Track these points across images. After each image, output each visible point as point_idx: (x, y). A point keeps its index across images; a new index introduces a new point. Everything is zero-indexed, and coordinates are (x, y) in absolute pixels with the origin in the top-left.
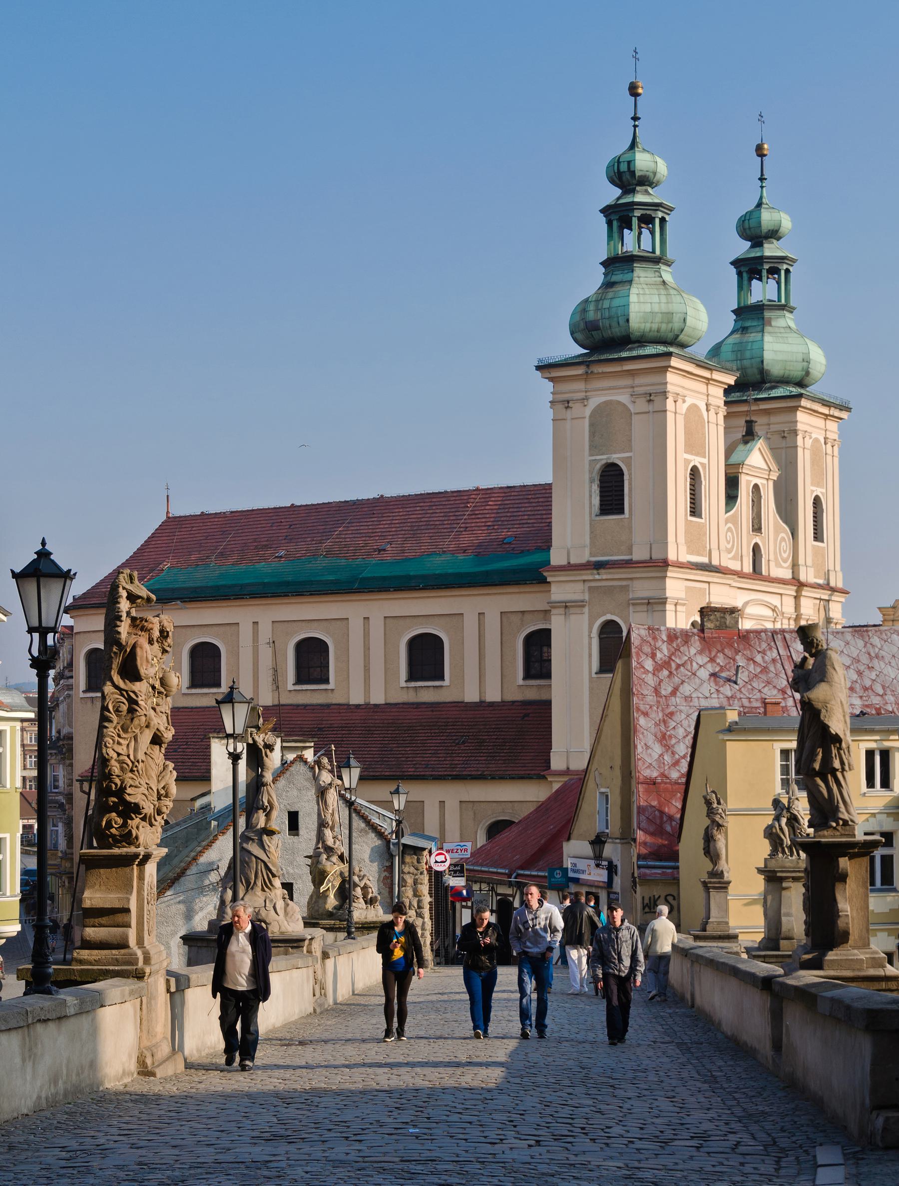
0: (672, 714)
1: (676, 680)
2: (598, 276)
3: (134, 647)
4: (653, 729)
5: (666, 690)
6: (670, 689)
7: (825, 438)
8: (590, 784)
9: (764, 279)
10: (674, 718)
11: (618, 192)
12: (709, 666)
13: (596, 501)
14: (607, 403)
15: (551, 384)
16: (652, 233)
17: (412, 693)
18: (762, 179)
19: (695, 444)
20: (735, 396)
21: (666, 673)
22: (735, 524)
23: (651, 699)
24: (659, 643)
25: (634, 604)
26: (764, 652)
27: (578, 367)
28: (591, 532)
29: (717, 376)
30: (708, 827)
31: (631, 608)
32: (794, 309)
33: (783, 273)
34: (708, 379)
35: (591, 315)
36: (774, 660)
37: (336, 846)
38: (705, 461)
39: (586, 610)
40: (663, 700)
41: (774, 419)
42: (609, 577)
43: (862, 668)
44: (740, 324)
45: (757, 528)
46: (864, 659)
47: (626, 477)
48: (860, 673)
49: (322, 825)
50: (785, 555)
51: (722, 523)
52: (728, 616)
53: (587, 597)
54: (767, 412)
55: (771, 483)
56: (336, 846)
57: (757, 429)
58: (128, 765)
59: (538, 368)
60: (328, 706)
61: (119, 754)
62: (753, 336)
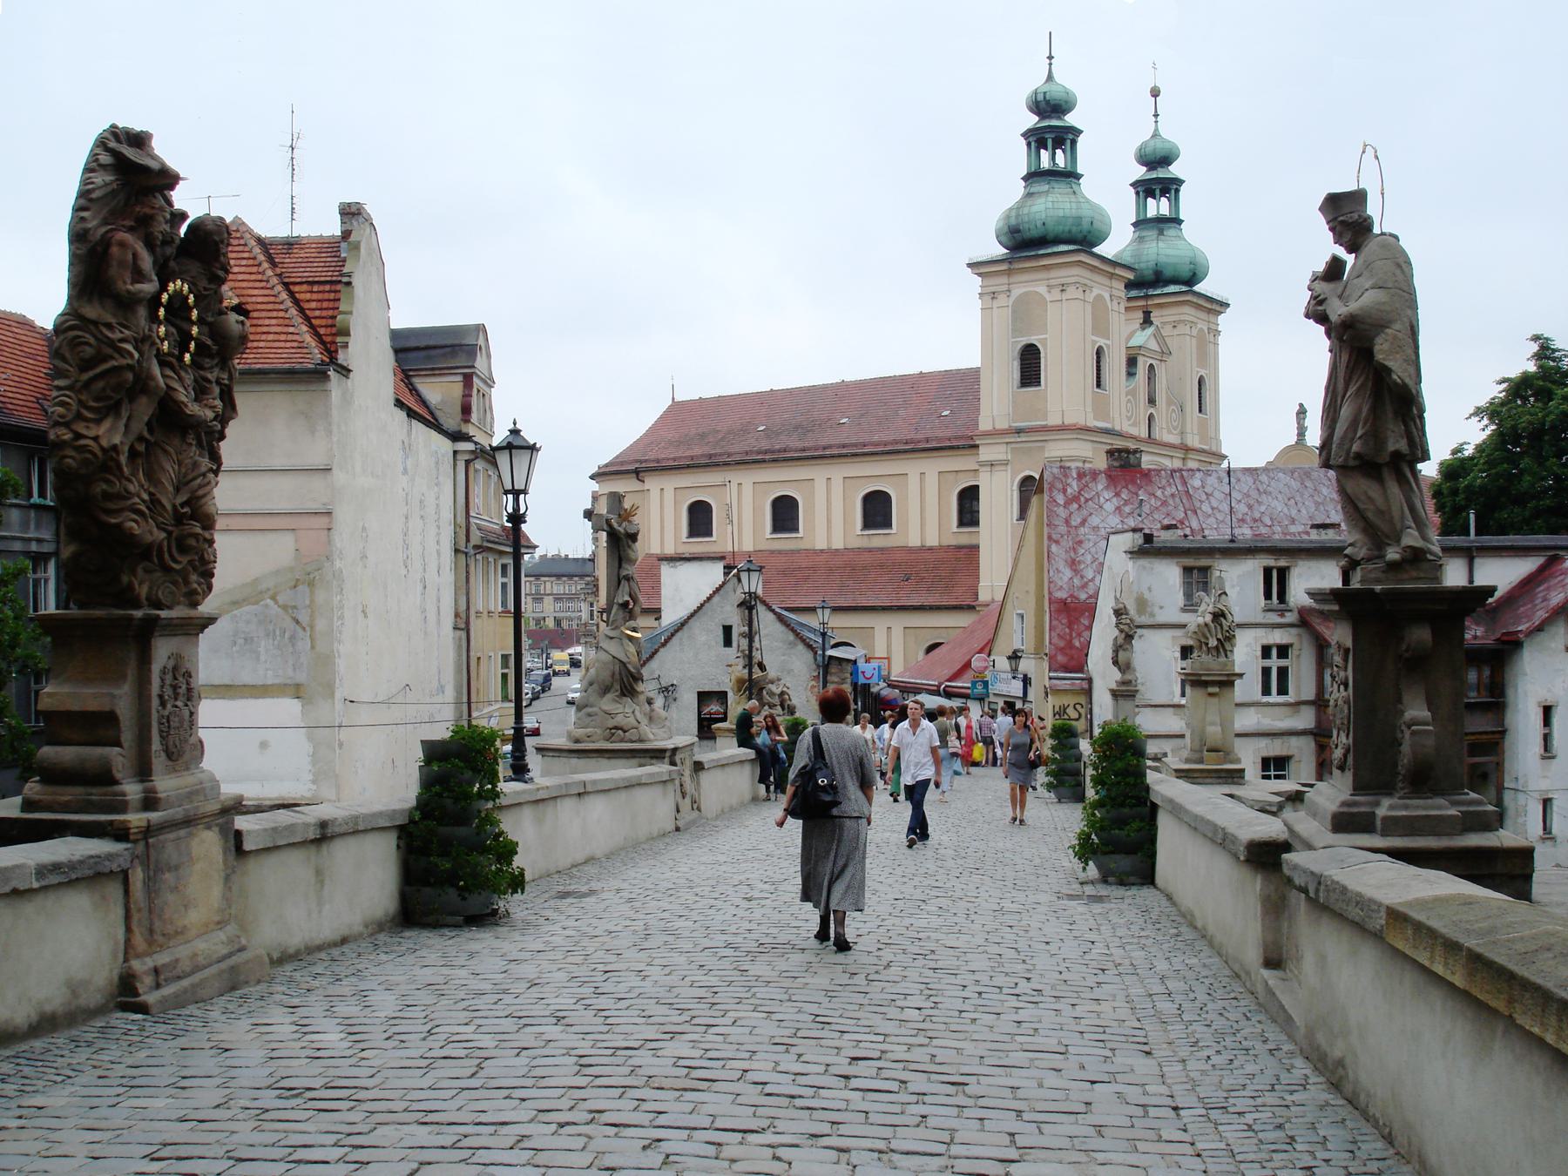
0: (1080, 542)
1: (1085, 512)
2: (1019, 189)
3: (106, 242)
4: (1063, 555)
5: (1076, 521)
6: (1079, 520)
7: (1209, 329)
8: (1009, 606)
9: (1158, 197)
10: (1083, 545)
11: (1036, 118)
12: (1115, 500)
13: (1017, 375)
14: (1026, 294)
15: (980, 279)
16: (1064, 151)
17: (866, 538)
18: (1156, 115)
19: (1100, 327)
20: (1134, 293)
21: (1075, 506)
22: (1134, 396)
23: (1063, 529)
24: (1070, 481)
26: (1163, 488)
29: (1119, 271)
33: (1173, 192)
34: (1112, 274)
35: (1013, 221)
36: (1173, 495)
38: (1107, 342)
39: (1009, 467)
40: (1072, 531)
43: (1252, 502)
45: (1152, 401)
46: (1254, 494)
47: (1042, 355)
48: (1250, 507)
50: (1175, 424)
52: (1131, 456)
58: (94, 455)
59: (969, 265)
60: (799, 551)
61: (78, 436)
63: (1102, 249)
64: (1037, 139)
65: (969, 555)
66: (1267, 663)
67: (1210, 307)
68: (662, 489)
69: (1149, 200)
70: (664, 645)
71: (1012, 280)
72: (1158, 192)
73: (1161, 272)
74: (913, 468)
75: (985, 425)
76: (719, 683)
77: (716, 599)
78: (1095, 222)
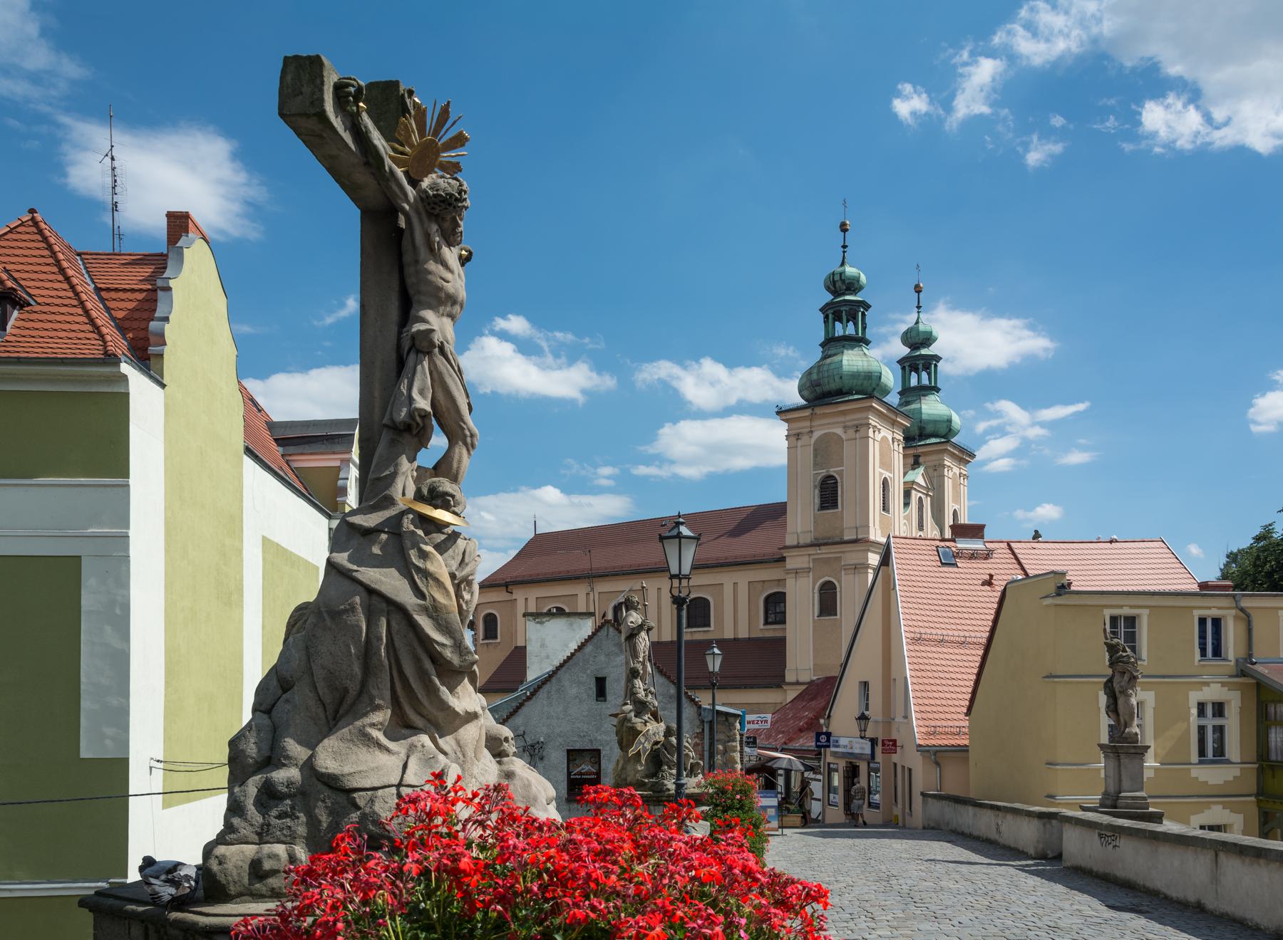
2: (818, 354)
7: (960, 473)
9: (921, 370)
13: (817, 501)
14: (825, 434)
19: (887, 465)
25: (845, 569)
27: (807, 410)
28: (815, 522)
30: (1110, 681)
31: (843, 572)
32: (940, 389)
35: (815, 376)
37: (649, 699)
38: (892, 476)
41: (928, 458)
42: (827, 551)
44: (904, 400)
47: (839, 484)
49: (634, 674)
51: (902, 518)
53: (811, 566)
54: (925, 454)
55: (929, 498)
56: (649, 699)
57: (921, 460)
62: (913, 406)
63: (887, 399)
64: (833, 313)
65: (778, 645)
66: (1203, 722)
67: (961, 455)
68: (526, 599)
69: (913, 373)
70: (529, 698)
71: (813, 424)
72: (920, 366)
73: (924, 428)
74: (727, 579)
75: (790, 540)
76: (591, 741)
77: (589, 648)
78: (882, 380)
